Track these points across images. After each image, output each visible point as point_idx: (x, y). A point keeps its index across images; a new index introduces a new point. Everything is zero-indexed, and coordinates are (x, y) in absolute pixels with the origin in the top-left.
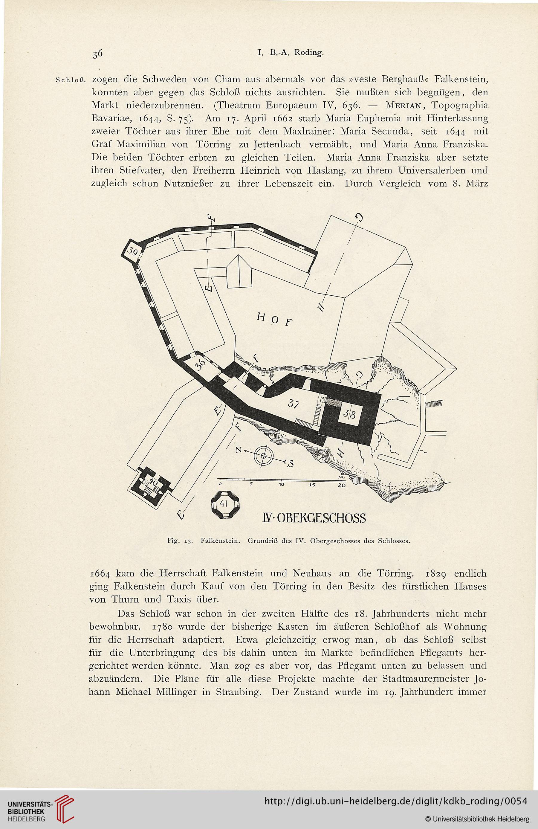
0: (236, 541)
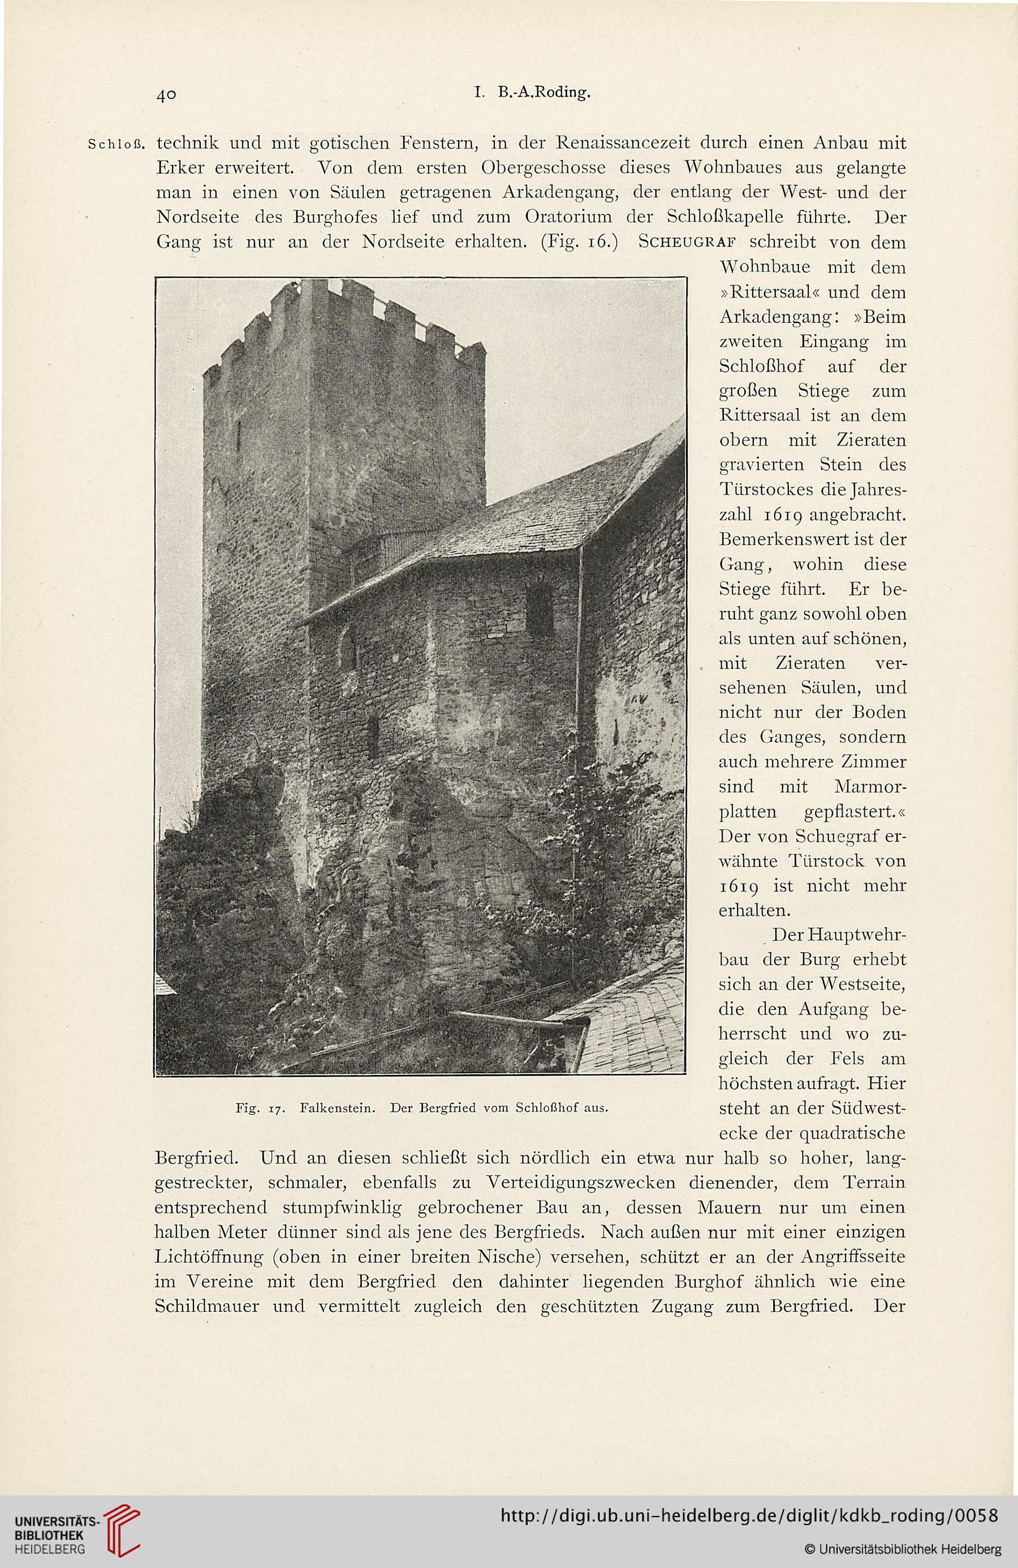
0: (368, 1109)
